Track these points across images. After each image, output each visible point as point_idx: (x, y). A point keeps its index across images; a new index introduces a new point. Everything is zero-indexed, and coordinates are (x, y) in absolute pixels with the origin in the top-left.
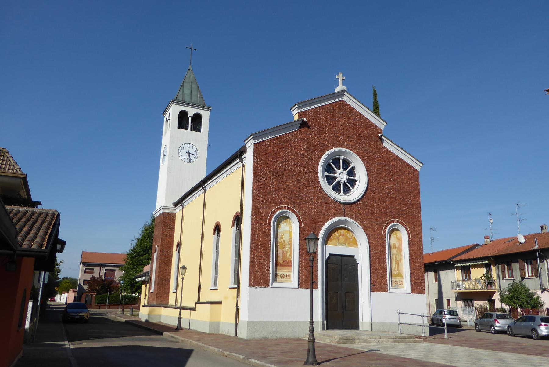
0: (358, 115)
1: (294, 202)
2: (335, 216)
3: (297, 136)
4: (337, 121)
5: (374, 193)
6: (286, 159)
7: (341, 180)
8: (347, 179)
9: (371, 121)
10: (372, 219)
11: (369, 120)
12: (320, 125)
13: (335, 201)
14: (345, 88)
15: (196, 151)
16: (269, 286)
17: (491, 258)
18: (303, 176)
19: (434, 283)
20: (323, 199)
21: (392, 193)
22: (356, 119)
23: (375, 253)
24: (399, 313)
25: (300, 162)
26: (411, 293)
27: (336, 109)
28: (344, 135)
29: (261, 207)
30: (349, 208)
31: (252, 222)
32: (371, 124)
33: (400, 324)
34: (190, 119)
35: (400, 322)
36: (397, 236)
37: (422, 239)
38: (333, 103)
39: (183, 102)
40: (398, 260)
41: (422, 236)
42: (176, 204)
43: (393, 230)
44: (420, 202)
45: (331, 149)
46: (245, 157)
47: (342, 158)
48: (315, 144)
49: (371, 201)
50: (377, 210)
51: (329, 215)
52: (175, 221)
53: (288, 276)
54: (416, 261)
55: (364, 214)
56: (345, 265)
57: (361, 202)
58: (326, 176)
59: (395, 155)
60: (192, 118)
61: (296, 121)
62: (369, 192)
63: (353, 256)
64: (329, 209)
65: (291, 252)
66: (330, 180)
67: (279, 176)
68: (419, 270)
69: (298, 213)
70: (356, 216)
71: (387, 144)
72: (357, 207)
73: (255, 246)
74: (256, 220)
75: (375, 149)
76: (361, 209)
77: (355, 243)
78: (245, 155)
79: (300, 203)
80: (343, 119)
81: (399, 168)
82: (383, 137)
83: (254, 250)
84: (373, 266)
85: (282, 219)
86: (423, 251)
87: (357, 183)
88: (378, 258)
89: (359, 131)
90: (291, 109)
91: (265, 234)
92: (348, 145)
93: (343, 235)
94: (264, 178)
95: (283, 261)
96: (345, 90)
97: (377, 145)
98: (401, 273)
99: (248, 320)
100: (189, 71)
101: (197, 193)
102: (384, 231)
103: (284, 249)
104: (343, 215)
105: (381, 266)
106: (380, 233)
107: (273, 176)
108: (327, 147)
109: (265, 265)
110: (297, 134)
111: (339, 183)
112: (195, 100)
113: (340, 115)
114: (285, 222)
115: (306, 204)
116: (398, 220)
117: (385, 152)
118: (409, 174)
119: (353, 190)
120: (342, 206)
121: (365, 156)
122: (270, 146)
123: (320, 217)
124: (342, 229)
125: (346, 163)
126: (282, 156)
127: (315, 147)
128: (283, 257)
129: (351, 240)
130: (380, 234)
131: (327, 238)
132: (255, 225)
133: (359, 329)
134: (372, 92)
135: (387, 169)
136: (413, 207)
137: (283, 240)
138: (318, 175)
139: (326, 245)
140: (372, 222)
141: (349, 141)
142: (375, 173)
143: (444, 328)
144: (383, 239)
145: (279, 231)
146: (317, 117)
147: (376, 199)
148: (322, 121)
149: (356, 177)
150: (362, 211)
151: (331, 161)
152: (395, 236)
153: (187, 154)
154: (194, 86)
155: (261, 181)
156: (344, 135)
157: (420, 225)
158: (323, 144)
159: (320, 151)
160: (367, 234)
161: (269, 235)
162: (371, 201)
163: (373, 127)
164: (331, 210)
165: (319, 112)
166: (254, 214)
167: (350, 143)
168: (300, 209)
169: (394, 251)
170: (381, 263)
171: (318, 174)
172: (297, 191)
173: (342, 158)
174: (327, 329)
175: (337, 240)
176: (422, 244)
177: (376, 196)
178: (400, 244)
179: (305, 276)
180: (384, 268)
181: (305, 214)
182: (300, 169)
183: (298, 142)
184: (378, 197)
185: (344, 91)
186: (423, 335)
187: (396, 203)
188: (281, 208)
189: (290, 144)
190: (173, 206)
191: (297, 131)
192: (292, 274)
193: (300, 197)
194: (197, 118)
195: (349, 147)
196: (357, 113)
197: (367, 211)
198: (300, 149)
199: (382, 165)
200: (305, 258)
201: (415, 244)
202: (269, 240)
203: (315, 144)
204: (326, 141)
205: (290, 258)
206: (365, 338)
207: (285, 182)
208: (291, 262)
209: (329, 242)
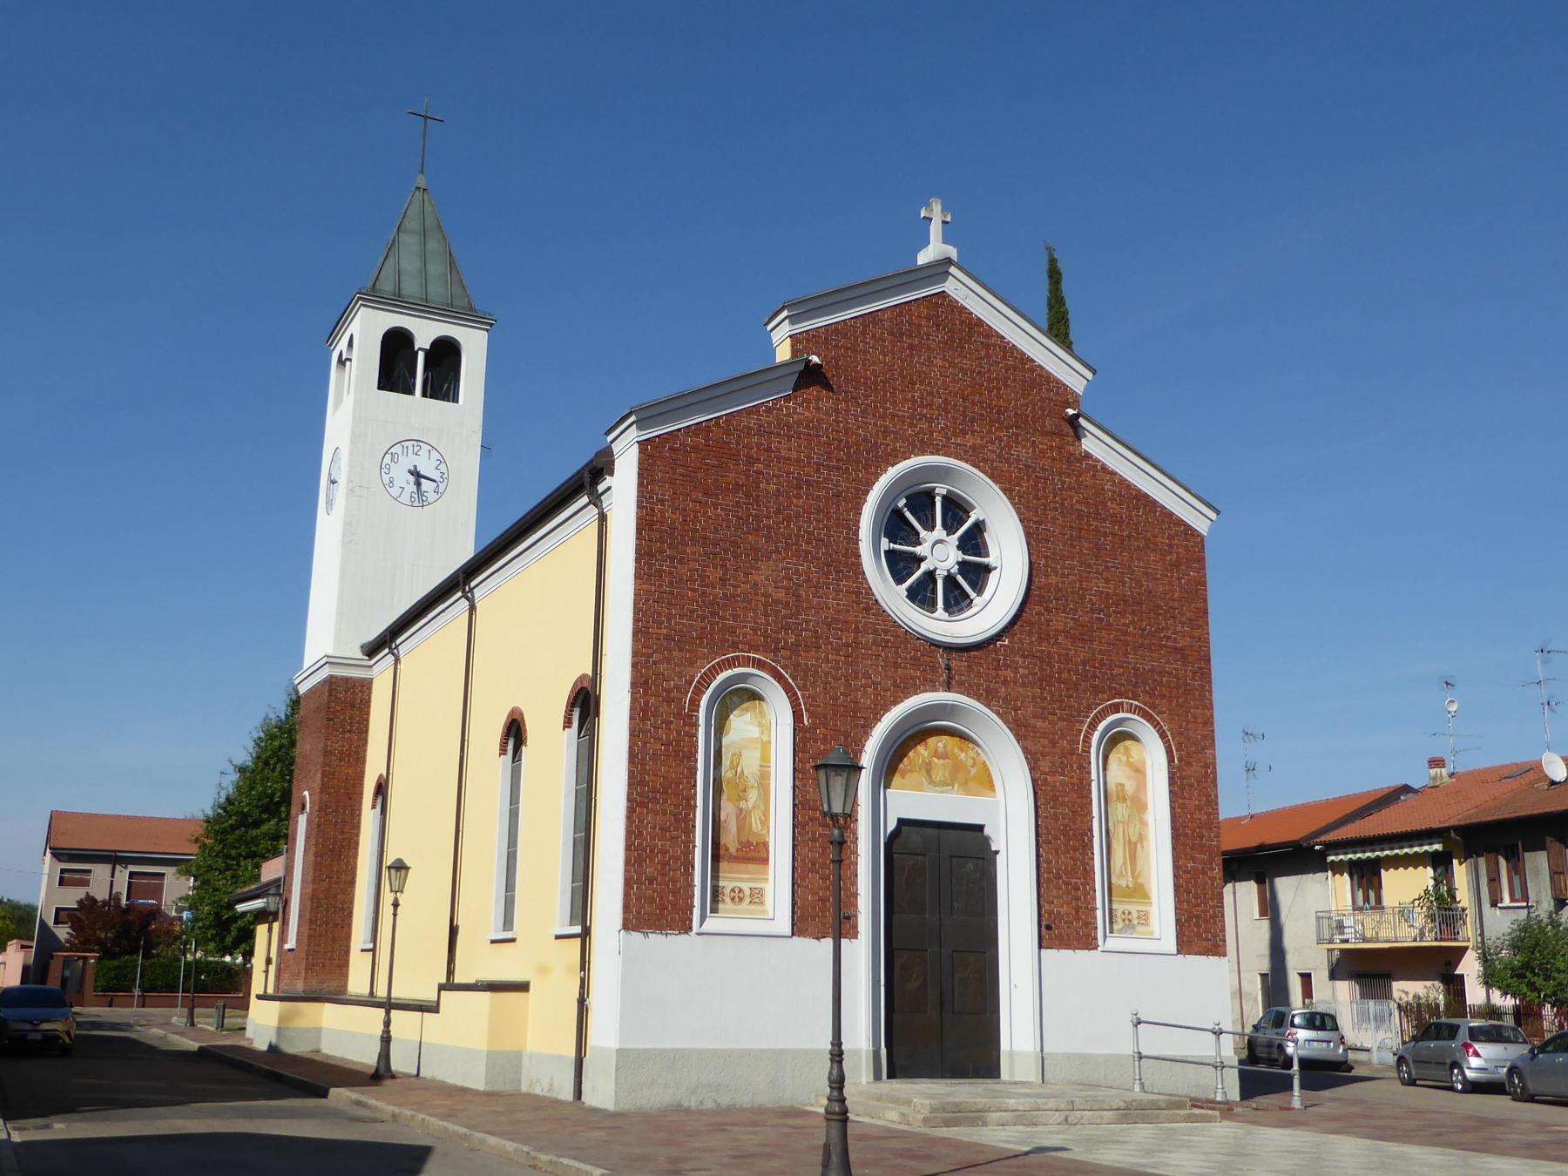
0: (994, 345)
1: (777, 641)
2: (916, 690)
3: (788, 415)
4: (923, 364)
5: (1049, 610)
6: (747, 496)
7: (939, 565)
8: (958, 563)
9: (1040, 366)
10: (1043, 699)
11: (1035, 362)
12: (867, 379)
13: (918, 638)
14: (953, 252)
15: (443, 468)
16: (691, 928)
17: (1453, 834)
18: (807, 552)
19: (1257, 917)
20: (875, 632)
21: (1114, 612)
22: (988, 356)
24: (1135, 1021)
25: (797, 506)
26: (1179, 952)
27: (920, 325)
28: (947, 413)
29: (665, 658)
30: (966, 664)
31: (632, 709)
32: (1041, 376)
33: (1141, 1058)
34: (421, 357)
35: (1140, 1053)
36: (1131, 760)
37: (1215, 768)
38: (911, 301)
39: (396, 301)
40: (1134, 839)
41: (1214, 758)
42: (372, 650)
43: (1116, 739)
44: (1207, 641)
45: (905, 459)
46: (609, 488)
47: (941, 489)
48: (847, 442)
50: (1060, 668)
51: (895, 685)
52: (369, 706)
53: (757, 897)
54: (1194, 845)
55: (1015, 683)
56: (952, 856)
57: (1006, 643)
58: (886, 552)
59: (1123, 481)
60: (429, 354)
61: (784, 365)
63: (980, 828)
64: (896, 665)
65: (766, 813)
66: (901, 565)
67: (726, 551)
68: (1204, 873)
69: (790, 680)
70: (988, 691)
71: (1095, 444)
72: (994, 659)
73: (644, 791)
74: (646, 703)
75: (1054, 459)
76: (1007, 666)
77: (984, 782)
78: (608, 481)
80: (944, 359)
81: (1137, 524)
82: (1081, 420)
83: (642, 805)
84: (1049, 862)
85: (735, 699)
86: (1217, 809)
87: (993, 577)
89: (999, 397)
90: (767, 324)
91: (677, 753)
92: (960, 445)
93: (944, 756)
94: (672, 558)
95: (740, 843)
96: (952, 258)
97: (1060, 448)
98: (1141, 886)
99: (618, 1047)
100: (419, 195)
101: (443, 611)
102: (1084, 741)
103: (742, 804)
104: (945, 685)
105: (1075, 861)
106: (1072, 749)
107: (706, 553)
108: (888, 455)
109: (677, 859)
110: (787, 407)
111: (930, 576)
112: (437, 291)
113: (933, 345)
114: (747, 710)
116: (1132, 704)
117: (1087, 470)
118: (1170, 545)
119: (978, 601)
120: (942, 657)
121: (1019, 485)
122: (695, 448)
123: (866, 692)
124: (941, 735)
125: (956, 510)
126: (737, 484)
127: (848, 455)
128: (739, 829)
129: (973, 771)
130: (1072, 752)
131: (890, 765)
132: (644, 719)
133: (998, 1076)
136: (1185, 658)
137: (739, 770)
138: (858, 549)
139: (885, 788)
140: (1044, 708)
141: (964, 433)
142: (1053, 543)
143: (1291, 1072)
144: (1081, 767)
145: (725, 740)
146: (854, 351)
147: (1057, 631)
148: (874, 363)
150: (1009, 674)
151: (902, 503)
152: (1124, 759)
153: (412, 479)
154: (433, 245)
155: (665, 571)
156: (947, 413)
157: (1209, 722)
158: (876, 443)
159: (866, 467)
160: (1025, 751)
161: (692, 756)
163: (1048, 383)
164: (905, 668)
165: (863, 333)
166: (641, 683)
167: (970, 440)
168: (797, 666)
169: (1119, 811)
170: (1075, 850)
171: (858, 544)
172: (787, 604)
173: (941, 489)
174: (891, 1075)
175: (924, 772)
176: (1216, 786)
177: (1059, 622)
178: (1141, 785)
179: (814, 894)
180: (1085, 869)
181: (814, 684)
182: (799, 529)
183: (789, 437)
184: (1065, 623)
185: (948, 261)
186: (1219, 1098)
187: (1127, 644)
188: (731, 663)
189: (762, 444)
190: (360, 656)
191: (787, 398)
193: (798, 624)
194: (445, 355)
195: (965, 452)
196: (992, 336)
197: (1026, 672)
198: (798, 461)
199: (1079, 515)
200: (814, 833)
201: (1191, 785)
202: (693, 772)
203: (847, 442)
204: (886, 432)
205: (764, 832)
206: (1021, 1108)
207: (747, 575)
208: (765, 845)
209: (897, 779)
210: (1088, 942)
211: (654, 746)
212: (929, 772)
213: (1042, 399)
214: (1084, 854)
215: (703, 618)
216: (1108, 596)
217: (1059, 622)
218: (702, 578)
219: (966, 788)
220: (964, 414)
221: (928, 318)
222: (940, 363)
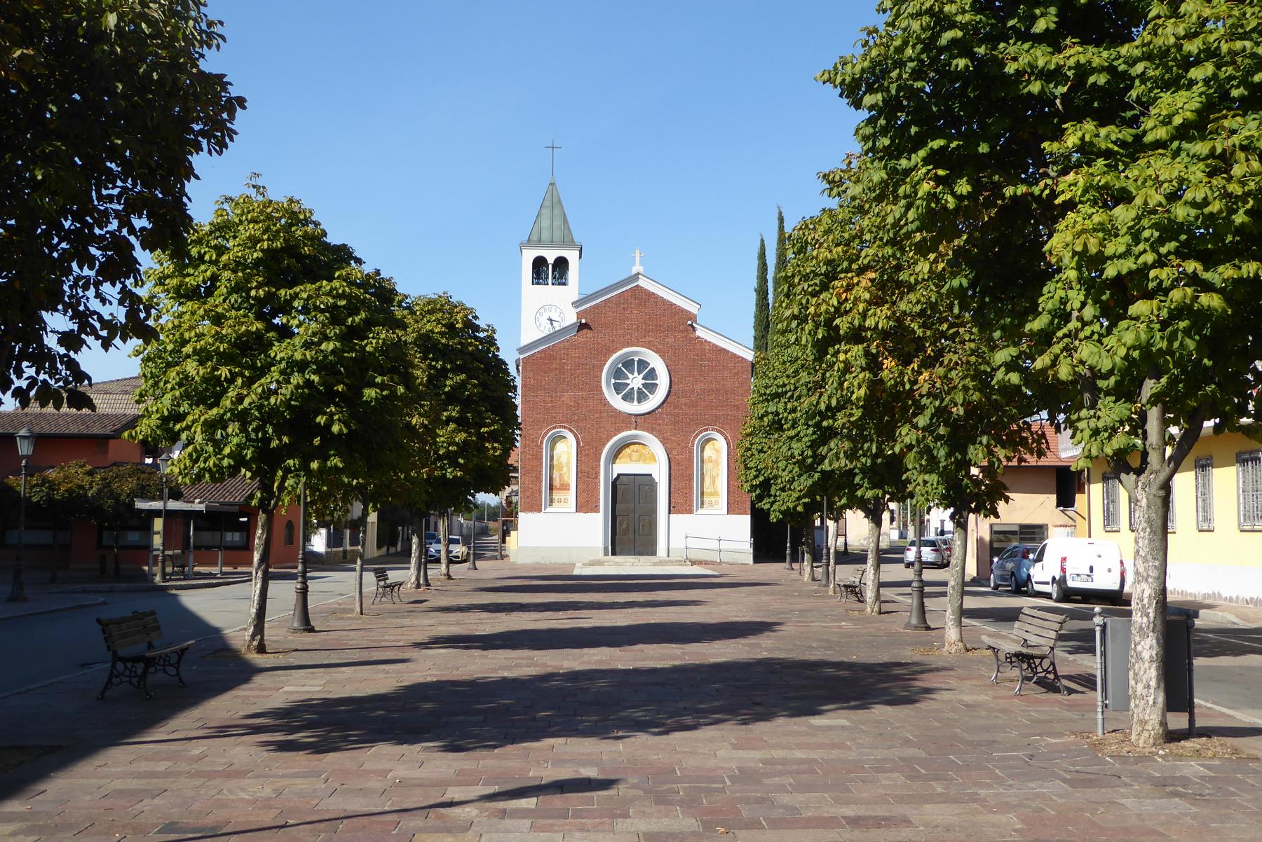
5: (678, 397)
15: (562, 315)
22: (656, 306)
23: (678, 470)
34: (550, 267)
39: (539, 244)
43: (709, 440)
47: (636, 359)
49: (675, 408)
53: (566, 501)
62: (671, 399)
63: (651, 475)
64: (615, 423)
71: (701, 333)
77: (653, 458)
89: (661, 321)
93: (637, 452)
97: (686, 337)
100: (551, 187)
115: (586, 420)
125: (643, 364)
130: (687, 447)
131: (616, 454)
133: (654, 553)
135: (701, 365)
136: (738, 409)
141: (645, 337)
150: (661, 422)
151: (620, 366)
153: (549, 322)
154: (557, 212)
161: (541, 458)
167: (647, 339)
168: (578, 427)
173: (636, 359)
177: (683, 401)
185: (638, 274)
188: (554, 428)
191: (575, 336)
192: (569, 498)
194: (561, 264)
202: (542, 463)
209: (618, 460)
210: (690, 511)
211: (528, 456)
215: (544, 414)
216: (705, 389)
217: (683, 401)
219: (645, 461)
220: (645, 330)
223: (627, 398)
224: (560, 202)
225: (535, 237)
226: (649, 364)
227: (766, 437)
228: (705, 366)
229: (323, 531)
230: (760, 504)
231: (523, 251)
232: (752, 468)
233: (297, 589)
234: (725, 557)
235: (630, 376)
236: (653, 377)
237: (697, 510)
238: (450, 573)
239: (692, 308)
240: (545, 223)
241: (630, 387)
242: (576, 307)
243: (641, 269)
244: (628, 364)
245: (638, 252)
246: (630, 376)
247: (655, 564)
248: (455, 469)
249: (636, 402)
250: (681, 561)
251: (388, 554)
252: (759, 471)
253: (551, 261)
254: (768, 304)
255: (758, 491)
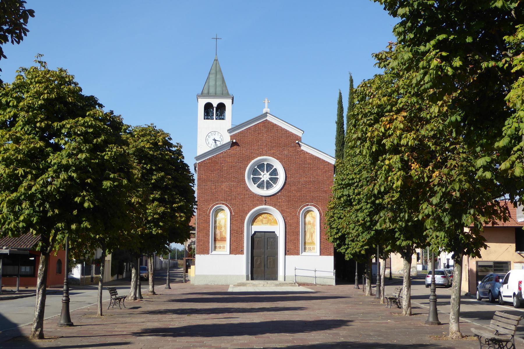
5: (291, 186)
6: (220, 171)
7: (267, 179)
10: (288, 205)
15: (222, 137)
22: (277, 132)
23: (291, 229)
43: (308, 211)
47: (265, 163)
49: (288, 192)
53: (224, 247)
59: (311, 155)
62: (287, 186)
63: (274, 232)
64: (253, 201)
65: (226, 232)
70: (275, 204)
71: (304, 148)
75: (293, 153)
77: (276, 222)
79: (231, 199)
80: (266, 135)
88: (293, 232)
89: (280, 141)
93: (266, 218)
97: (295, 150)
100: (215, 62)
113: (263, 132)
115: (236, 199)
118: (324, 168)
125: (269, 166)
127: (243, 159)
128: (221, 235)
130: (295, 215)
131: (253, 220)
132: (200, 216)
134: (349, 79)
135: (304, 167)
139: (252, 225)
141: (271, 150)
144: (297, 218)
149: (278, 175)
150: (280, 200)
151: (256, 167)
153: (214, 141)
154: (218, 76)
161: (209, 222)
162: (288, 192)
165: (247, 132)
167: (272, 151)
168: (231, 203)
173: (265, 163)
177: (293, 188)
178: (314, 221)
181: (235, 207)
183: (230, 157)
185: (267, 113)
188: (217, 204)
191: (229, 149)
192: (226, 246)
194: (221, 107)
204: (252, 153)
209: (255, 223)
210: (298, 254)
211: (201, 221)
212: (262, 222)
213: (291, 139)
214: (298, 236)
218: (211, 188)
219: (271, 224)
220: (271, 146)
221: (263, 126)
222: (265, 135)
223: (260, 186)
224: (220, 71)
225: (206, 92)
226: (273, 166)
227: (342, 210)
228: (306, 168)
229: (79, 266)
230: (339, 249)
231: (199, 99)
232: (334, 228)
233: (63, 300)
234: (319, 281)
235: (262, 173)
236: (275, 174)
237: (302, 253)
238: (155, 291)
239: (299, 133)
240: (212, 83)
241: (262, 180)
242: (230, 133)
243: (268, 110)
244: (261, 166)
245: (266, 100)
246: (262, 173)
247: (277, 285)
248: (157, 229)
249: (265, 189)
250: (292, 283)
251: (118, 279)
252: (338, 230)
253: (215, 105)
254: (344, 131)
255: (338, 242)
